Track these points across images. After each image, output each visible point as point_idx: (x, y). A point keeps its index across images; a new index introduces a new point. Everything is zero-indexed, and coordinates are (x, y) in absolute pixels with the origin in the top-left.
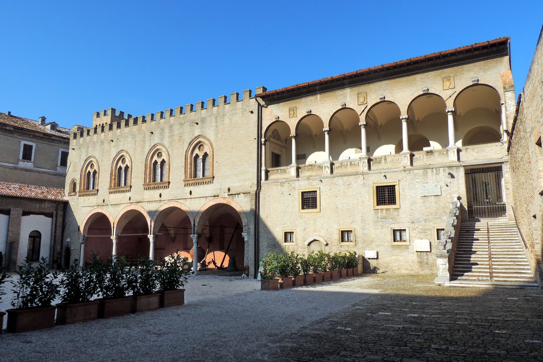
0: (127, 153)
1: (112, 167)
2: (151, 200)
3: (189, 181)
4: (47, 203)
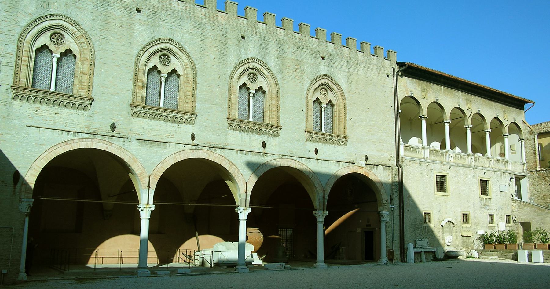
0: (181, 48)
1: (137, 62)
3: (315, 133)
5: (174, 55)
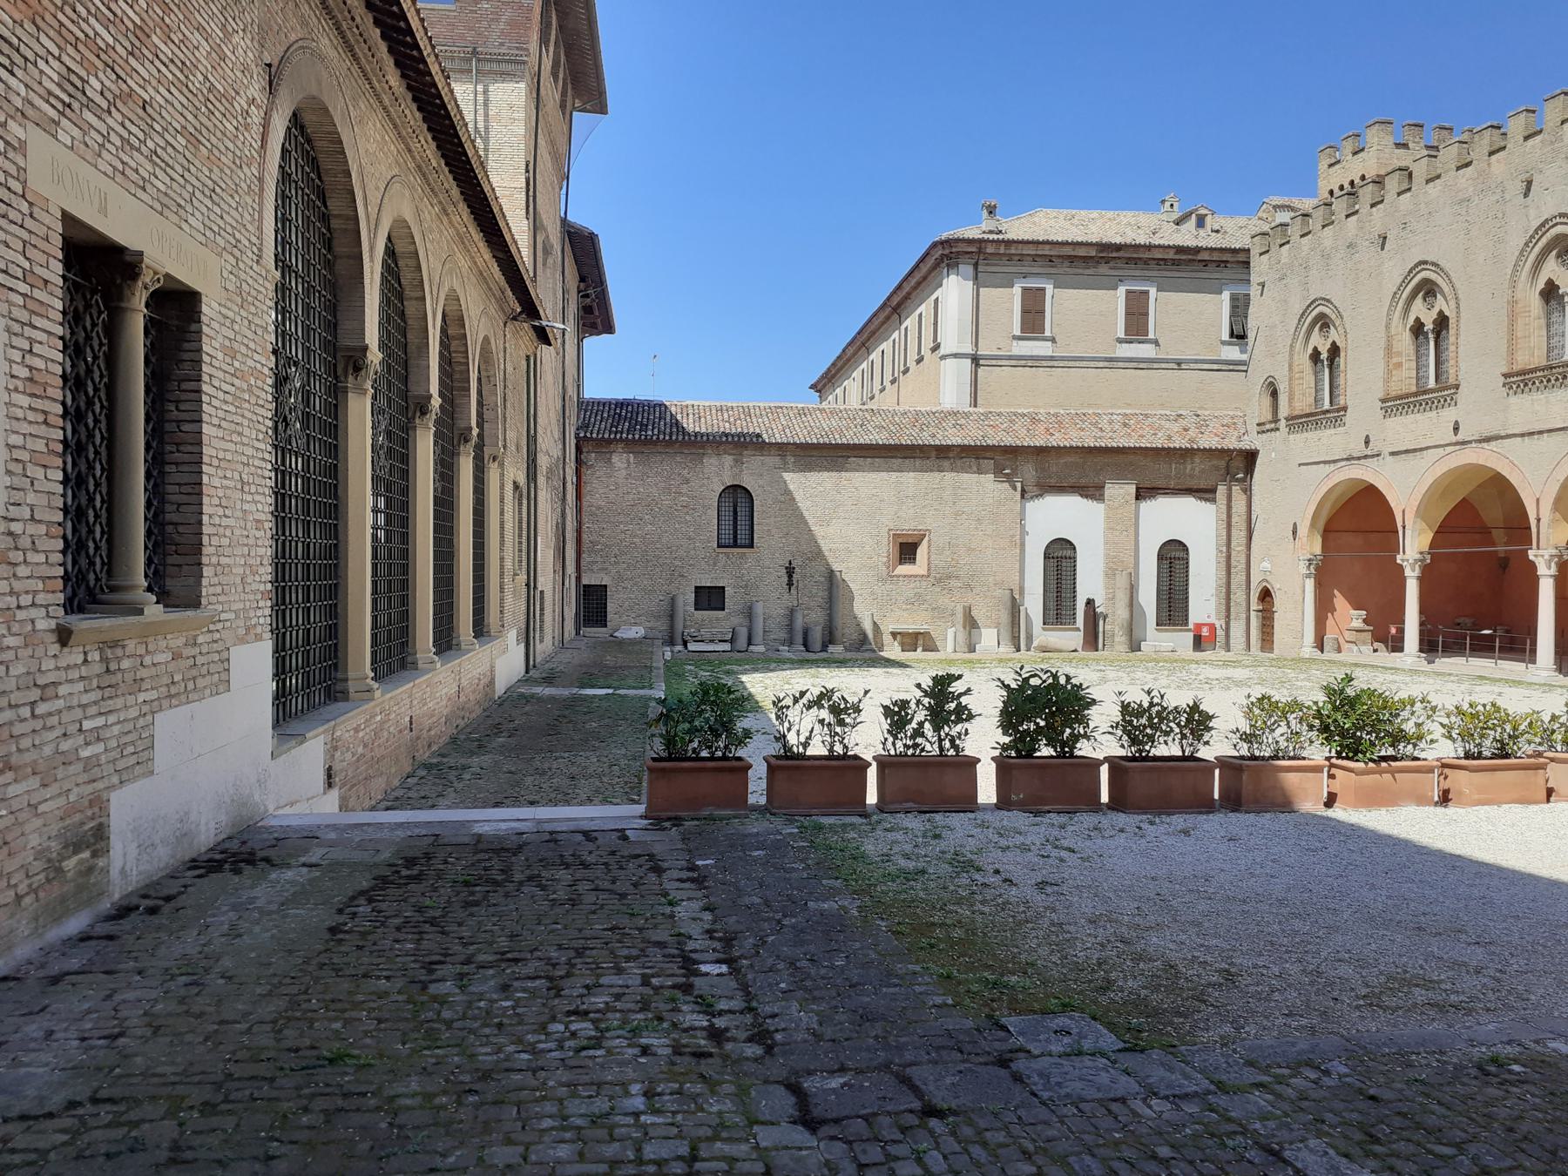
1: (1388, 327)
2: (1538, 428)
4: (1197, 460)
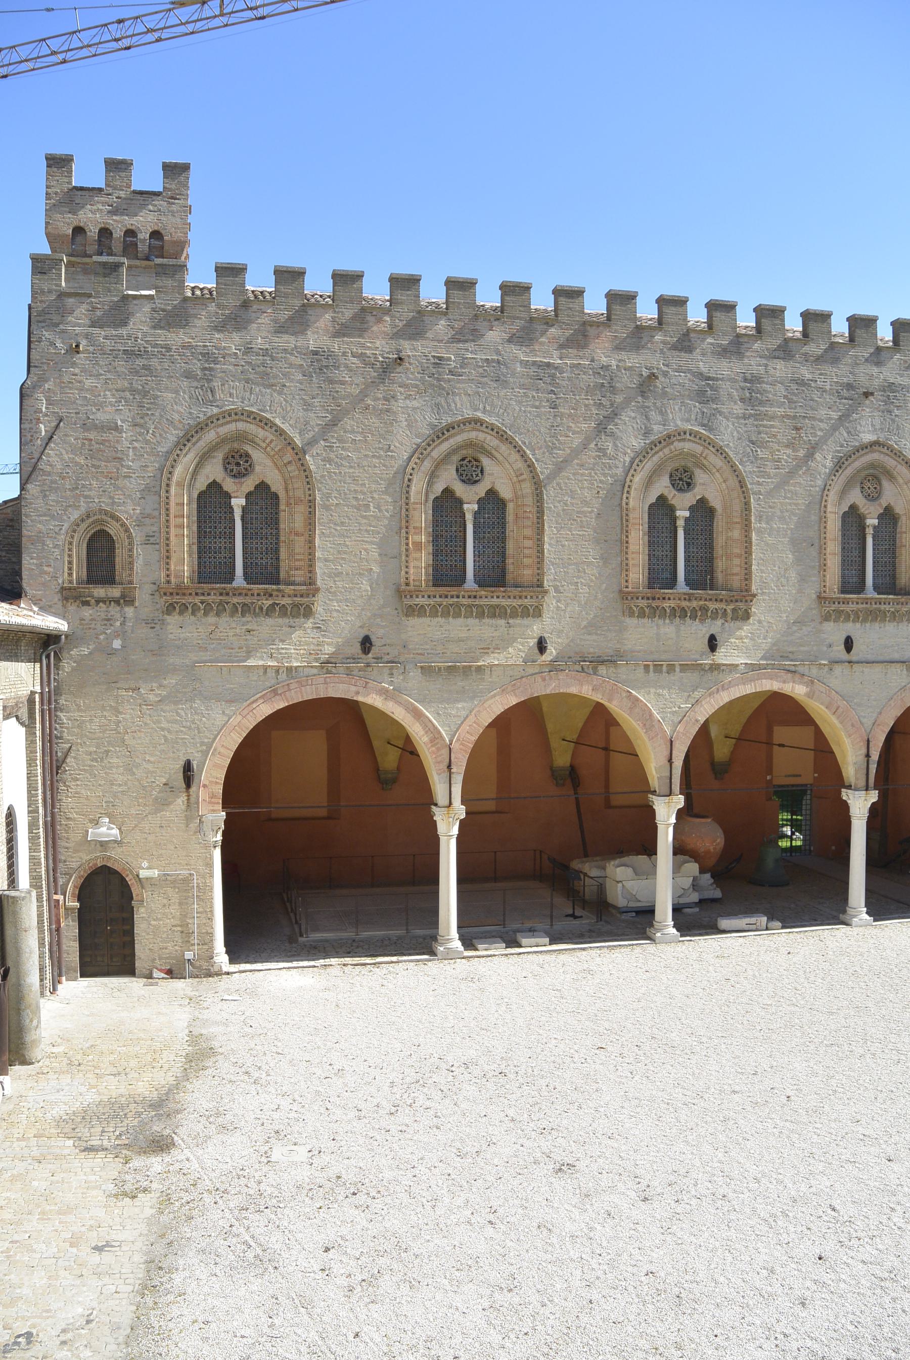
0: (502, 436)
5: (490, 455)
